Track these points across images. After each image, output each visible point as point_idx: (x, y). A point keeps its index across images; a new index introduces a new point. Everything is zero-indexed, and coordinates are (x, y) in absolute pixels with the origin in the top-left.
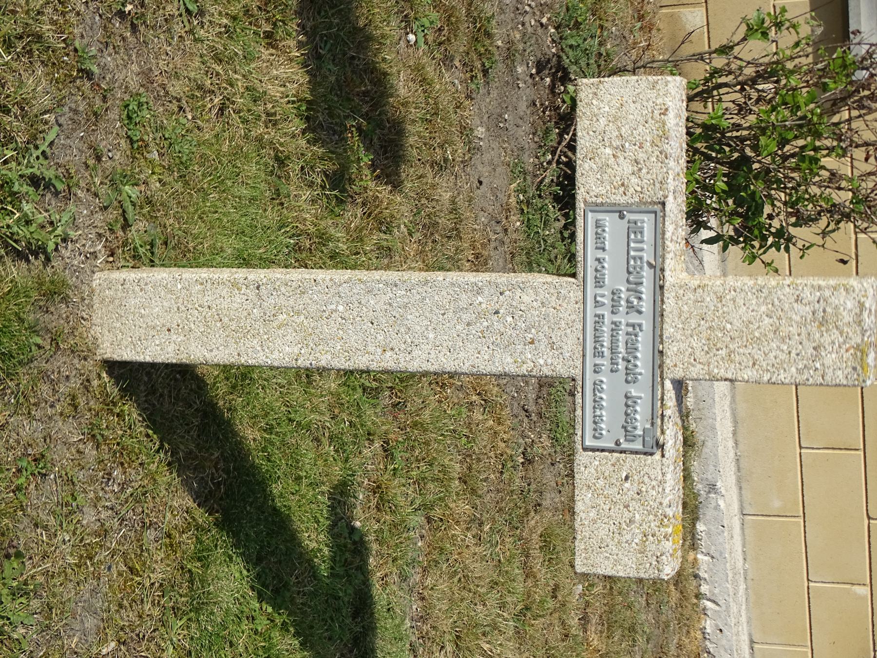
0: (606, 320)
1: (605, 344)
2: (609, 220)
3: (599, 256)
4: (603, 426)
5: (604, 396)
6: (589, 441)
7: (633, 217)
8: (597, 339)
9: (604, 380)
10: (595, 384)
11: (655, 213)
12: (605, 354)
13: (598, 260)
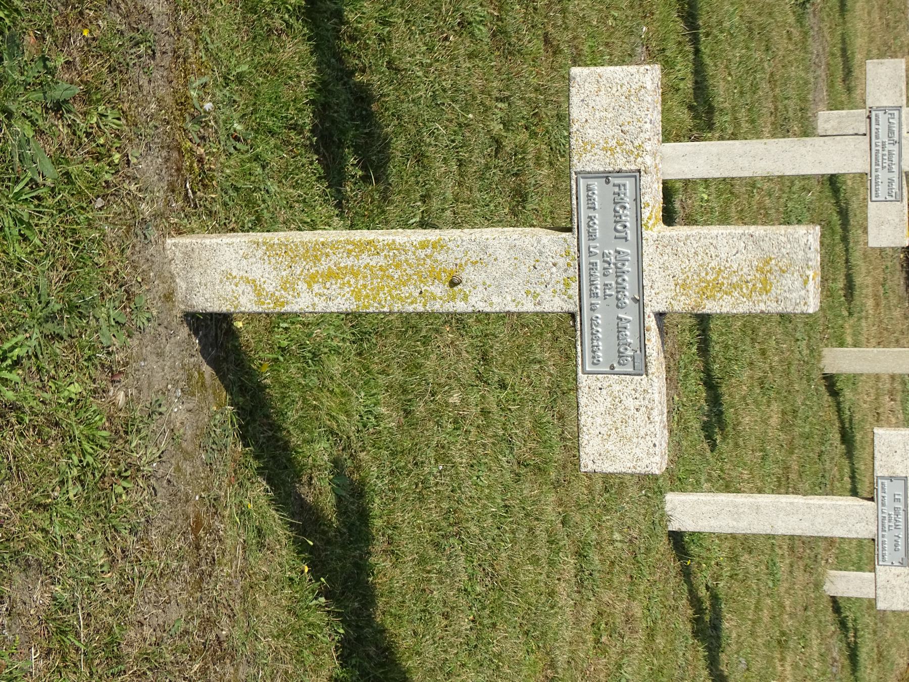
0: (598, 267)
1: (599, 286)
2: (596, 184)
3: (590, 215)
4: (600, 354)
5: (600, 330)
6: (589, 367)
7: (617, 181)
8: (591, 283)
9: (599, 316)
10: (592, 319)
11: (635, 177)
12: (599, 295)
13: (590, 217)
